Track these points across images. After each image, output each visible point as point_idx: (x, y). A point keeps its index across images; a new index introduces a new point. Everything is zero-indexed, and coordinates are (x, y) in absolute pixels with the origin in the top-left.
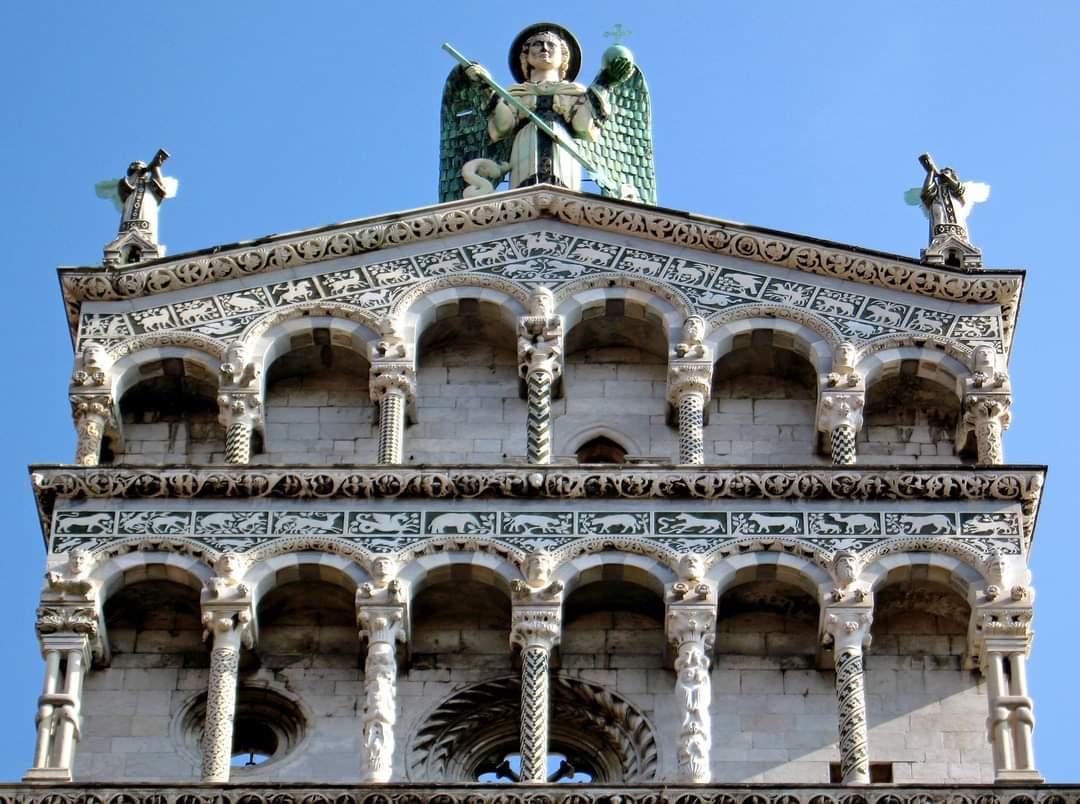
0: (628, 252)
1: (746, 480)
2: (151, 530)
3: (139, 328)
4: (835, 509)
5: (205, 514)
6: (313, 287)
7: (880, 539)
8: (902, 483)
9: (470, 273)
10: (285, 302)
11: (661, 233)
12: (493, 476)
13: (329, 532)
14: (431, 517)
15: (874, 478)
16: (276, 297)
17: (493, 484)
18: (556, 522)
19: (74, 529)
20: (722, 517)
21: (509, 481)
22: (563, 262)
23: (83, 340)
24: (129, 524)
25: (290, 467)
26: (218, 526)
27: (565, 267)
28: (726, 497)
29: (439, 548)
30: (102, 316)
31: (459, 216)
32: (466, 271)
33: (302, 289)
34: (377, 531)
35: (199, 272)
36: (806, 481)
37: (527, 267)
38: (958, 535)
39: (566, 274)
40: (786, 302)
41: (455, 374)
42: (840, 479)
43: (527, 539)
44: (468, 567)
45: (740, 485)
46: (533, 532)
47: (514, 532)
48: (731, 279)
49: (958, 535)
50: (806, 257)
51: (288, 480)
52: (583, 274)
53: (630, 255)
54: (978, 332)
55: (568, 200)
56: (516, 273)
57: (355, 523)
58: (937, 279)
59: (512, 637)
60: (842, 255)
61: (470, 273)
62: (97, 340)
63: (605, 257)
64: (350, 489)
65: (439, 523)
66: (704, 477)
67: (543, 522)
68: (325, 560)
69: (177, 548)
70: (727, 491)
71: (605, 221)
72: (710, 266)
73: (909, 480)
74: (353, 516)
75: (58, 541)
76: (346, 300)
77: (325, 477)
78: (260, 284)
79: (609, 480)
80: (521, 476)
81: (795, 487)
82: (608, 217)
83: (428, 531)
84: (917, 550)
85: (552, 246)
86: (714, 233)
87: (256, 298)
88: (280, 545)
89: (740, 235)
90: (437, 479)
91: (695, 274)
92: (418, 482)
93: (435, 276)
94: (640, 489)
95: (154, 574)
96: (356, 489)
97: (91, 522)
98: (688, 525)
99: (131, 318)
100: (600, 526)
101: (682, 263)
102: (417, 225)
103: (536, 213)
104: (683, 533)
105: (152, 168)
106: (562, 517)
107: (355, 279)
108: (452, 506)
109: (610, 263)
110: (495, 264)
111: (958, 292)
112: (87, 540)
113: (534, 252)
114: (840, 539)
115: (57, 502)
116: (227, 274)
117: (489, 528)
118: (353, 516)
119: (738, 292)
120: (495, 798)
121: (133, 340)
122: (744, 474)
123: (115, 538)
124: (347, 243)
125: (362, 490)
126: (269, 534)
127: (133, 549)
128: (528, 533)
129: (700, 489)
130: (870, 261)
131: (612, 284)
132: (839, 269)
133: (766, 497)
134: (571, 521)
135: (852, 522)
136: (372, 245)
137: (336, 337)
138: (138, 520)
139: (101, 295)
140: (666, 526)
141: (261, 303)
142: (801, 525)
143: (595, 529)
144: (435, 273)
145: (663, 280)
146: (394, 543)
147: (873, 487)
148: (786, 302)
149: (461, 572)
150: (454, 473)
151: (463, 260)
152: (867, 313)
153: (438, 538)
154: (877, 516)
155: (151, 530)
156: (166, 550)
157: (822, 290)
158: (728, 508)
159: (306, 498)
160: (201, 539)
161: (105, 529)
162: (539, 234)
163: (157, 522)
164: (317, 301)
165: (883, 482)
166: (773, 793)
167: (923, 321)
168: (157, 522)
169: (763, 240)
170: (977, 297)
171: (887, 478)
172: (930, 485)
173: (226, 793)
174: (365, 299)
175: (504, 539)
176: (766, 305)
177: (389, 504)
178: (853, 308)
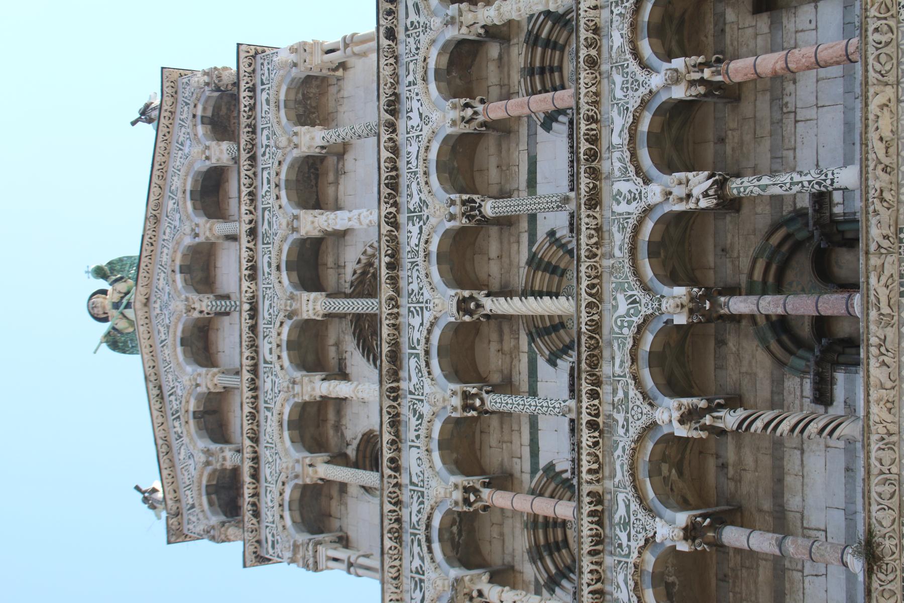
3: (193, 506)
9: (169, 342)
11: (152, 248)
12: (245, 329)
14: (266, 362)
19: (273, 547)
25: (242, 434)
28: (255, 208)
29: (279, 357)
33: (177, 424)
36: (246, 167)
37: (167, 313)
40: (178, 184)
41: (220, 349)
42: (245, 150)
44: (288, 342)
45: (248, 202)
58: (166, 110)
59: (319, 318)
60: (157, 159)
61: (169, 342)
63: (163, 275)
64: (253, 403)
65: (268, 358)
67: (267, 303)
68: (286, 417)
69: (281, 494)
70: (251, 208)
71: (147, 275)
72: (164, 224)
73: (245, 114)
74: (266, 402)
75: (278, 556)
76: (180, 403)
78: (175, 444)
79: (246, 269)
80: (245, 315)
81: (250, 173)
82: (145, 274)
83: (271, 363)
84: (278, 107)
85: (159, 301)
88: (278, 440)
91: (168, 230)
95: (296, 506)
96: (253, 400)
99: (189, 509)
100: (269, 274)
103: (146, 309)
105: (143, 493)
107: (173, 398)
108: (261, 350)
111: (172, 100)
115: (262, 555)
118: (266, 402)
121: (197, 510)
122: (242, 199)
125: (253, 397)
127: (282, 517)
128: (271, 311)
129: (251, 222)
130: (159, 144)
131: (173, 271)
132: (164, 159)
133: (255, 188)
135: (265, 142)
137: (198, 407)
138: (269, 513)
139: (179, 524)
142: (266, 168)
145: (171, 246)
146: (277, 380)
147: (248, 132)
149: (291, 346)
150: (244, 350)
152: (182, 144)
153: (274, 358)
154: (263, 129)
156: (283, 500)
158: (260, 207)
159: (258, 426)
166: (382, 172)
168: (270, 504)
172: (247, 103)
173: (386, 476)
176: (180, 195)
177: (260, 383)
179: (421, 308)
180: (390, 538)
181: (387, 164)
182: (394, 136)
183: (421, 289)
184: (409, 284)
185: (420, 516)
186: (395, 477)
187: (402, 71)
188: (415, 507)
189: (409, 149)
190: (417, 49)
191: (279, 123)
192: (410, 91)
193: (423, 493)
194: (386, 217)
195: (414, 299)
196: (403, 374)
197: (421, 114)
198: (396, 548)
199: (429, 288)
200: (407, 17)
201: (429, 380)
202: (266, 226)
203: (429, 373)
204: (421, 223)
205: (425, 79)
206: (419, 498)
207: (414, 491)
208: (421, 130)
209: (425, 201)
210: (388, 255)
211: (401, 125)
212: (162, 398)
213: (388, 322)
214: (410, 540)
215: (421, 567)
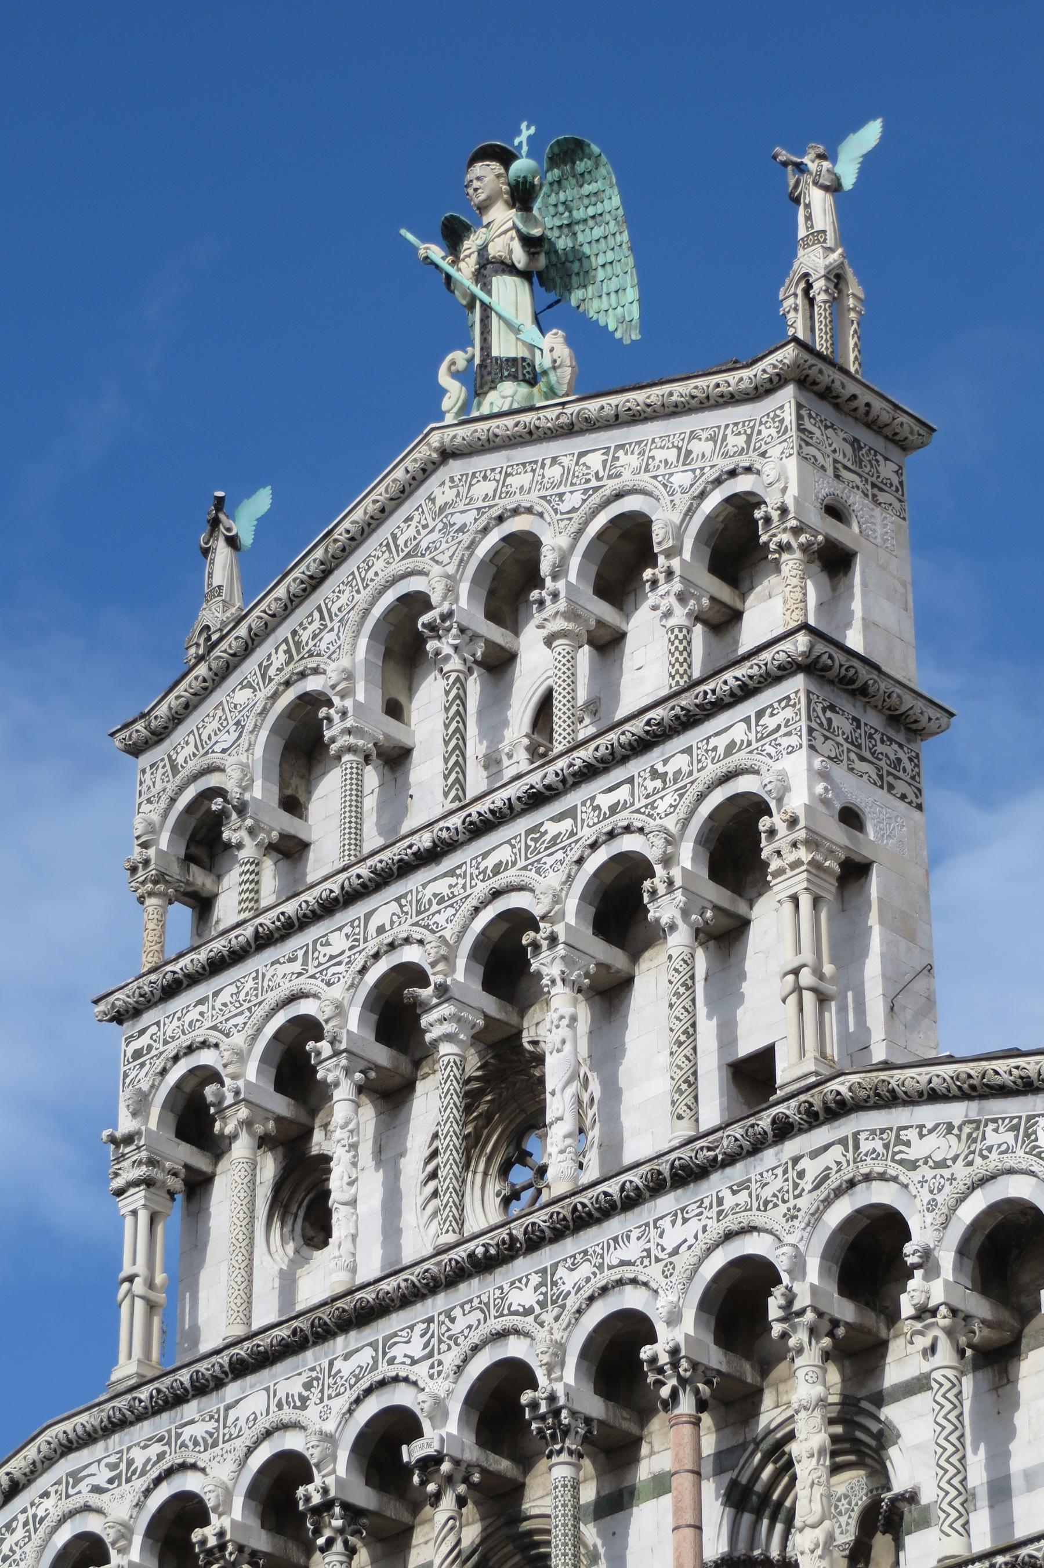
0: (509, 470)
1: (578, 763)
2: (184, 1033)
3: (175, 769)
4: (654, 758)
5: (216, 994)
6: (288, 651)
7: (692, 782)
8: (697, 701)
9: (399, 567)
10: (271, 680)
13: (300, 974)
14: (368, 916)
15: (673, 708)
16: (263, 676)
17: (401, 860)
18: (453, 880)
19: (138, 1054)
20: (571, 813)
21: (409, 851)
22: (462, 512)
23: (140, 804)
24: (169, 1033)
26: (225, 1005)
27: (459, 520)
30: (152, 766)
31: (375, 502)
32: (393, 566)
33: (282, 657)
34: (332, 958)
35: (205, 680)
36: (623, 738)
37: (435, 536)
38: (754, 745)
39: (462, 529)
42: (648, 723)
43: (433, 914)
46: (438, 904)
47: (426, 910)
48: (584, 464)
49: (754, 745)
50: (629, 409)
51: (260, 929)
52: (476, 520)
53: (511, 474)
54: (773, 431)
55: (452, 434)
56: (428, 548)
57: (316, 955)
62: (149, 801)
66: (545, 776)
67: (442, 887)
77: (283, 913)
86: (558, 418)
87: (251, 686)
89: (577, 409)
90: (359, 876)
91: (555, 472)
92: (346, 883)
93: (372, 584)
94: (506, 811)
97: (144, 1041)
98: (548, 837)
101: (548, 462)
102: (348, 532)
104: (547, 848)
106: (458, 872)
109: (495, 491)
110: (414, 543)
112: (142, 1065)
113: (442, 509)
114: (662, 798)
116: (228, 667)
117: (407, 913)
119: (588, 481)
120: (395, 1284)
122: (575, 754)
123: (161, 1053)
124: (302, 582)
126: (260, 999)
128: (435, 907)
129: (549, 787)
134: (465, 877)
136: (323, 571)
140: (532, 844)
141: (255, 690)
142: (632, 795)
143: (481, 877)
144: (372, 580)
147: (677, 717)
148: (627, 475)
150: (370, 862)
151: (390, 552)
153: (372, 947)
155: (184, 1033)
157: (653, 441)
160: (214, 1028)
161: (155, 1045)
162: (443, 483)
163: (187, 1019)
164: (291, 666)
165: (683, 709)
167: (732, 440)
168: (187, 1019)
169: (592, 407)
170: (768, 386)
171: (683, 703)
174: (323, 646)
175: (416, 924)
176: (611, 486)
178: (675, 451)
179: (430, 1355)
180: (151, 1397)
181: (602, 1196)
182: (648, 1194)
183: (457, 1345)
184: (462, 1306)
185: (191, 1445)
186: (225, 1373)
187: (737, 1172)
188: (199, 1430)
189: (634, 1236)
190: (766, 1203)
191: (701, 797)
192: (711, 1207)
193: (215, 1444)
194: (533, 1224)
195: (444, 1328)
196: (354, 1339)
197: (675, 1252)
198: (145, 1408)
199: (458, 1362)
200: (815, 1154)
201: (347, 1406)
202: (552, 829)
203: (358, 1401)
204: (537, 1309)
205: (729, 1236)
206: (211, 1435)
207: (218, 1421)
208: (658, 1260)
209: (563, 1307)
210: (487, 1251)
211: (667, 1203)
212: (314, 588)
213: (403, 1285)
214: (162, 1432)
215: (134, 1472)
